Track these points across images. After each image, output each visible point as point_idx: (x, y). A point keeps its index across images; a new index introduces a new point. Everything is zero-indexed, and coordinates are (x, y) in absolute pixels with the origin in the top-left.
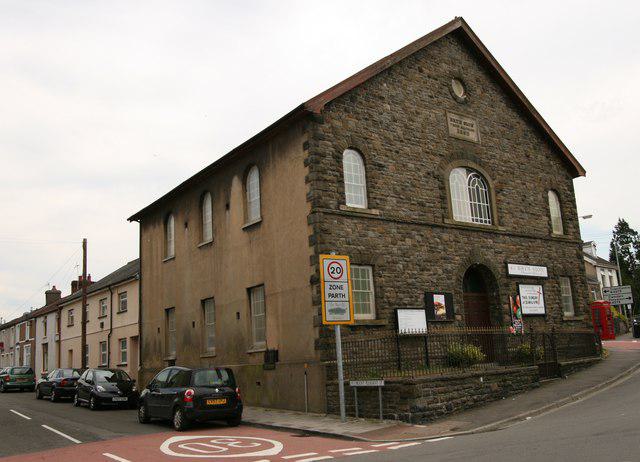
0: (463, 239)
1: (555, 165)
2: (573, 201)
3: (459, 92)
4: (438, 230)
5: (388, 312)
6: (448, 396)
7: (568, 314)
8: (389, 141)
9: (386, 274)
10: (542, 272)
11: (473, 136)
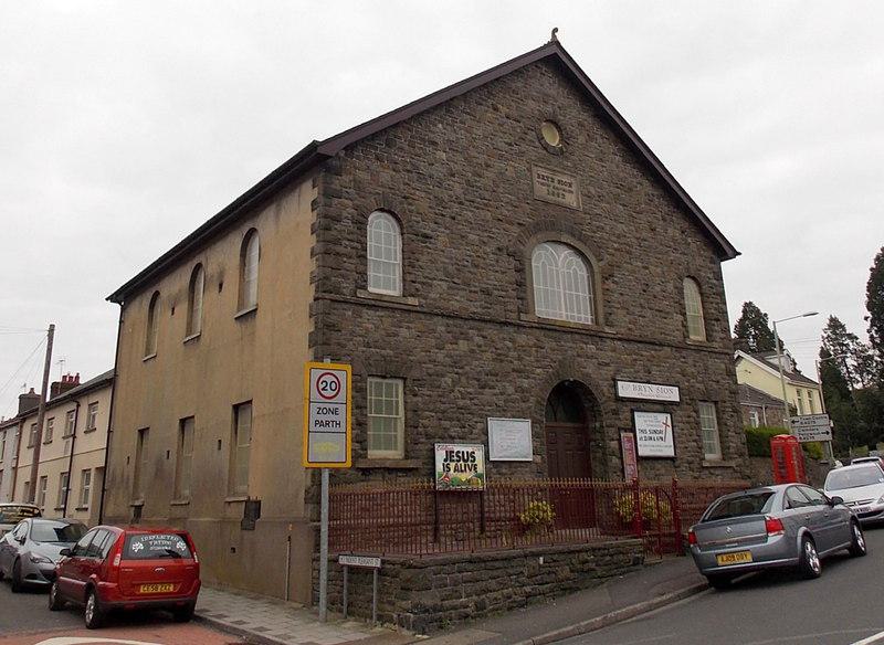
0: (549, 344)
1: (694, 243)
2: (722, 294)
3: (552, 139)
4: (511, 330)
5: (423, 448)
6: (478, 586)
7: (713, 456)
8: (440, 201)
9: (425, 391)
10: (672, 394)
11: (571, 200)
